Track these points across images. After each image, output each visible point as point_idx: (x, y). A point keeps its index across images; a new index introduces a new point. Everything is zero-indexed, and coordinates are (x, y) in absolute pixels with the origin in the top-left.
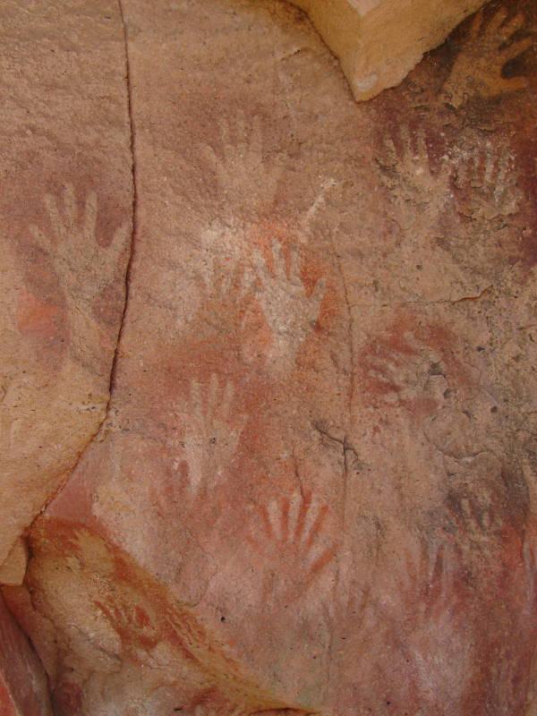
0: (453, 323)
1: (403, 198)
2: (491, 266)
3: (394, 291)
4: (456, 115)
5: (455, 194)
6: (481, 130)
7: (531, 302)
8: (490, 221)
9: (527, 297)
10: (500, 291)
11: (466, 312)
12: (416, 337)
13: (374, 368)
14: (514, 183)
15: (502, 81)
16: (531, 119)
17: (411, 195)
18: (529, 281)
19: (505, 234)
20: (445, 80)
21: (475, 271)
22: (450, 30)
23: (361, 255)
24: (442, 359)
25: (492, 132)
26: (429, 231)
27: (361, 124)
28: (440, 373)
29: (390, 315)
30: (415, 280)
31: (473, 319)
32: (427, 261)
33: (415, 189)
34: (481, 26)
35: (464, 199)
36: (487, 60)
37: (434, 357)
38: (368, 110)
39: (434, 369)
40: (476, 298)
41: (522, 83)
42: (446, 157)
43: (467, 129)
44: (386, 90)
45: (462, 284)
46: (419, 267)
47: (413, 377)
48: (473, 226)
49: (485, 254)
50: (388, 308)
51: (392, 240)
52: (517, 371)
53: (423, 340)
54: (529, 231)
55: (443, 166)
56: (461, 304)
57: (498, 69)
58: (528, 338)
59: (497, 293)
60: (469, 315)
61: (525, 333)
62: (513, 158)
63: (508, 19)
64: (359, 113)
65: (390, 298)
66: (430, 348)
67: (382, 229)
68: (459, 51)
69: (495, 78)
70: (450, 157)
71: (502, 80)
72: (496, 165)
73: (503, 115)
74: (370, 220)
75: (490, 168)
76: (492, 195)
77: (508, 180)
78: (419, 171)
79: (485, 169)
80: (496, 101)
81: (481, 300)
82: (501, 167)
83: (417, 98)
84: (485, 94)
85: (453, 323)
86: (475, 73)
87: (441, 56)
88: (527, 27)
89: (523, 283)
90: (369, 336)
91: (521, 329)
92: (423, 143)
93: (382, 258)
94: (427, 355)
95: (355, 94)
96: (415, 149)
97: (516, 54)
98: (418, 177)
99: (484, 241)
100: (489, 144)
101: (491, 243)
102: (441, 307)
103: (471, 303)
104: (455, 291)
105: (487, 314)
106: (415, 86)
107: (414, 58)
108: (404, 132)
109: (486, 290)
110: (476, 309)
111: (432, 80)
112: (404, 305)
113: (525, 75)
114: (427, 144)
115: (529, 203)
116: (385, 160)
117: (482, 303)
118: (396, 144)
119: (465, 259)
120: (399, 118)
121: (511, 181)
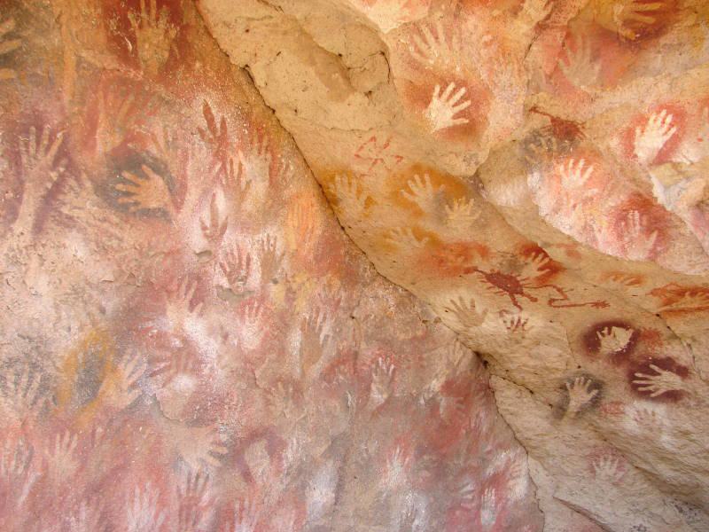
18: (9, 235)
54: (11, 195)
58: (5, 282)
88: (17, 31)
113: (15, 69)
115: (12, 172)
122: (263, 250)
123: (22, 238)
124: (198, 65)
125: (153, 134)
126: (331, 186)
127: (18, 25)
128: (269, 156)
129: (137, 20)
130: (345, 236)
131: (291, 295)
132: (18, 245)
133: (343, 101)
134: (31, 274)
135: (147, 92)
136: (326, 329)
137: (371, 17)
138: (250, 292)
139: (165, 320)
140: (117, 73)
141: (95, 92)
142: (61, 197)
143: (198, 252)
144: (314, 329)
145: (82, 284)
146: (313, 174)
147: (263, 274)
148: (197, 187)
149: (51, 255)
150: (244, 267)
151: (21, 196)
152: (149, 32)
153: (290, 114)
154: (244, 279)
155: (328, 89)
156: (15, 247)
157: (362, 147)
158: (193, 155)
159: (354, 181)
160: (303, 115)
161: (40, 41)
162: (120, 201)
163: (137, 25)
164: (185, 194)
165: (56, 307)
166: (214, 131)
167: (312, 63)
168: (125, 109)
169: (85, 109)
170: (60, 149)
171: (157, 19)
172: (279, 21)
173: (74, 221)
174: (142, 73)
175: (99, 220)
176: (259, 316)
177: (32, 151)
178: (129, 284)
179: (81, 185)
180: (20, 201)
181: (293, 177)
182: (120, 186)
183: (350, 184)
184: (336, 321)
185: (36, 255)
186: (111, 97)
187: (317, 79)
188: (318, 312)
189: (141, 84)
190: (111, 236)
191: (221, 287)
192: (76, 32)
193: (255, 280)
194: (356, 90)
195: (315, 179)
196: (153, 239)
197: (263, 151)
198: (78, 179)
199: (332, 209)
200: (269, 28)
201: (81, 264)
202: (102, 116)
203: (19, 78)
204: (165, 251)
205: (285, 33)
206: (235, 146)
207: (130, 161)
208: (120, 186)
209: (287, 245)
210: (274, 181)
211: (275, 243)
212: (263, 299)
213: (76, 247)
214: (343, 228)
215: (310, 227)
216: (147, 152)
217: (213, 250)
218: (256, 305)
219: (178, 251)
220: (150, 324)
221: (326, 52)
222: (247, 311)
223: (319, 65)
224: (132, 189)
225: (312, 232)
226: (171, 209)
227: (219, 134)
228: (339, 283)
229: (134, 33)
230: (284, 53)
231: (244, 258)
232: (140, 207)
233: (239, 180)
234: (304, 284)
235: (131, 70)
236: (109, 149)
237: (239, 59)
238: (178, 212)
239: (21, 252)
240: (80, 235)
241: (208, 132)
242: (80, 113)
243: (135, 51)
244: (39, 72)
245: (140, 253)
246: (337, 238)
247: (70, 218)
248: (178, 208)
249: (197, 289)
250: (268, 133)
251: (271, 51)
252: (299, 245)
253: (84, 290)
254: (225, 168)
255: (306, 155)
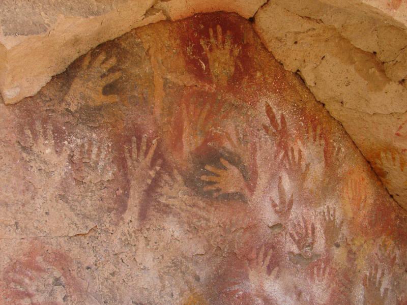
0: (70, 250)
1: (37, 168)
2: (96, 213)
3: (29, 230)
4: (73, 116)
5: (72, 166)
6: (89, 126)
7: (122, 237)
8: (95, 184)
9: (120, 234)
10: (101, 230)
11: (79, 243)
12: (44, 260)
13: (14, 281)
14: (111, 160)
15: (102, 96)
16: (121, 121)
17: (43, 166)
19: (105, 193)
20: (66, 94)
21: (85, 216)
22: (69, 63)
23: (7, 205)
24: (63, 275)
25: (96, 128)
26: (54, 190)
27: (9, 119)
28: (61, 284)
29: (26, 246)
30: (44, 222)
31: (83, 248)
32: (53, 209)
33: (45, 162)
34: (90, 62)
35: (77, 169)
36: (93, 83)
37: (57, 274)
38: (13, 110)
39: (57, 282)
40: (86, 234)
41: (115, 98)
42: (66, 142)
43: (80, 125)
44: (26, 98)
45: (76, 224)
46: (46, 213)
47: (42, 287)
48: (84, 187)
49: (92, 205)
50: (25, 241)
51: (28, 196)
52: (113, 282)
53: (49, 262)
54: (121, 191)
55: (64, 148)
56: (76, 238)
57: (100, 89)
59: (99, 231)
60: (80, 246)
61: (118, 257)
62: (110, 145)
63: (106, 59)
64: (7, 112)
65: (27, 234)
66: (54, 267)
67: (22, 188)
68: (76, 76)
69: (98, 95)
70: (69, 143)
71: (102, 96)
72: (99, 148)
73: (103, 117)
74: (14, 182)
75: (95, 150)
76: (97, 168)
77: (107, 159)
78: (48, 151)
79: (92, 151)
80: (99, 108)
81: (88, 236)
82: (102, 150)
83: (47, 104)
84: (91, 103)
85: (70, 250)
86: (86, 91)
87: (65, 77)
88: (118, 65)
89: (117, 225)
90: (11, 260)
91: (116, 254)
92: (51, 132)
93: (21, 207)
94: (52, 273)
95: (5, 99)
96: (45, 137)
97: (112, 81)
98: (47, 154)
99: (91, 197)
100: (94, 135)
101: (95, 199)
102: (62, 240)
103: (83, 238)
104: (71, 229)
105: (93, 245)
106: (46, 97)
107: (45, 79)
108: (38, 126)
109: (91, 229)
110: (86, 241)
111: (57, 94)
112: (36, 239)
113: (118, 94)
114: (53, 133)
115: (120, 174)
116: (25, 143)
117: (90, 237)
118: (32, 133)
119: (79, 209)
120: (35, 116)
121: (109, 159)
122: (325, 219)
123: (131, 225)
124: (259, 74)
125: (227, 133)
126: (378, 161)
127: (119, 61)
128: (323, 142)
129: (208, 45)
130: (394, 203)
131: (351, 255)
132: (128, 231)
133: (381, 90)
134: (139, 253)
135: (219, 100)
136: (385, 284)
137: (396, 18)
138: (316, 255)
139: (248, 283)
140: (195, 88)
141: (179, 105)
142: (159, 190)
143: (271, 225)
144: (374, 283)
145: (180, 258)
146: (362, 154)
147: (327, 240)
148: (265, 172)
149: (154, 236)
150: (310, 235)
151: (129, 192)
152: (217, 53)
153: (338, 106)
154: (311, 245)
155: (366, 82)
156: (127, 233)
157: (401, 127)
158: (261, 147)
159: (397, 156)
160: (347, 106)
161: (136, 71)
162: (205, 189)
163: (208, 49)
164: (256, 179)
165: (161, 278)
166: (276, 126)
167: (352, 63)
168: (204, 115)
169: (173, 119)
170: (156, 152)
171: (223, 42)
172: (321, 31)
173: (170, 208)
174: (214, 86)
175: (190, 206)
176: (326, 275)
177: (135, 156)
178: (217, 255)
179: (174, 179)
180: (127, 195)
181: (345, 157)
182: (204, 178)
183: (394, 158)
184: (393, 276)
185: (143, 237)
186: (192, 107)
187: (357, 75)
188: (376, 269)
189: (215, 94)
190: (200, 218)
191: (292, 253)
192: (162, 60)
193: (320, 245)
194: (391, 80)
195: (363, 156)
196: (234, 218)
197: (318, 139)
198: (170, 175)
199: (381, 181)
200: (313, 38)
201: (178, 242)
202: (186, 123)
203: (121, 101)
204: (244, 226)
205: (327, 41)
206: (294, 136)
207: (211, 156)
208: (204, 178)
209: (345, 214)
210: (329, 162)
211: (334, 213)
212: (328, 261)
213: (173, 228)
214: (391, 196)
215: (363, 197)
216: (224, 148)
217: (283, 222)
218: (323, 266)
219: (255, 226)
220: (236, 287)
221: (363, 52)
222: (315, 272)
223: (357, 63)
224: (214, 179)
225: (365, 201)
226: (246, 192)
227: (280, 128)
228: (393, 242)
229: (206, 54)
230: (328, 57)
231: (310, 227)
232: (221, 193)
233: (299, 164)
234: (362, 246)
235: (206, 84)
236: (193, 148)
237: (291, 65)
238: (252, 194)
239: (131, 235)
240: (176, 219)
241: (271, 127)
242: (169, 122)
243: (208, 69)
244: (136, 95)
245: (224, 229)
246: (388, 204)
247: (167, 206)
248: (252, 190)
249: (273, 256)
250: (321, 124)
251: (316, 56)
252: (355, 213)
253: (181, 262)
254: (287, 155)
255: (354, 137)
